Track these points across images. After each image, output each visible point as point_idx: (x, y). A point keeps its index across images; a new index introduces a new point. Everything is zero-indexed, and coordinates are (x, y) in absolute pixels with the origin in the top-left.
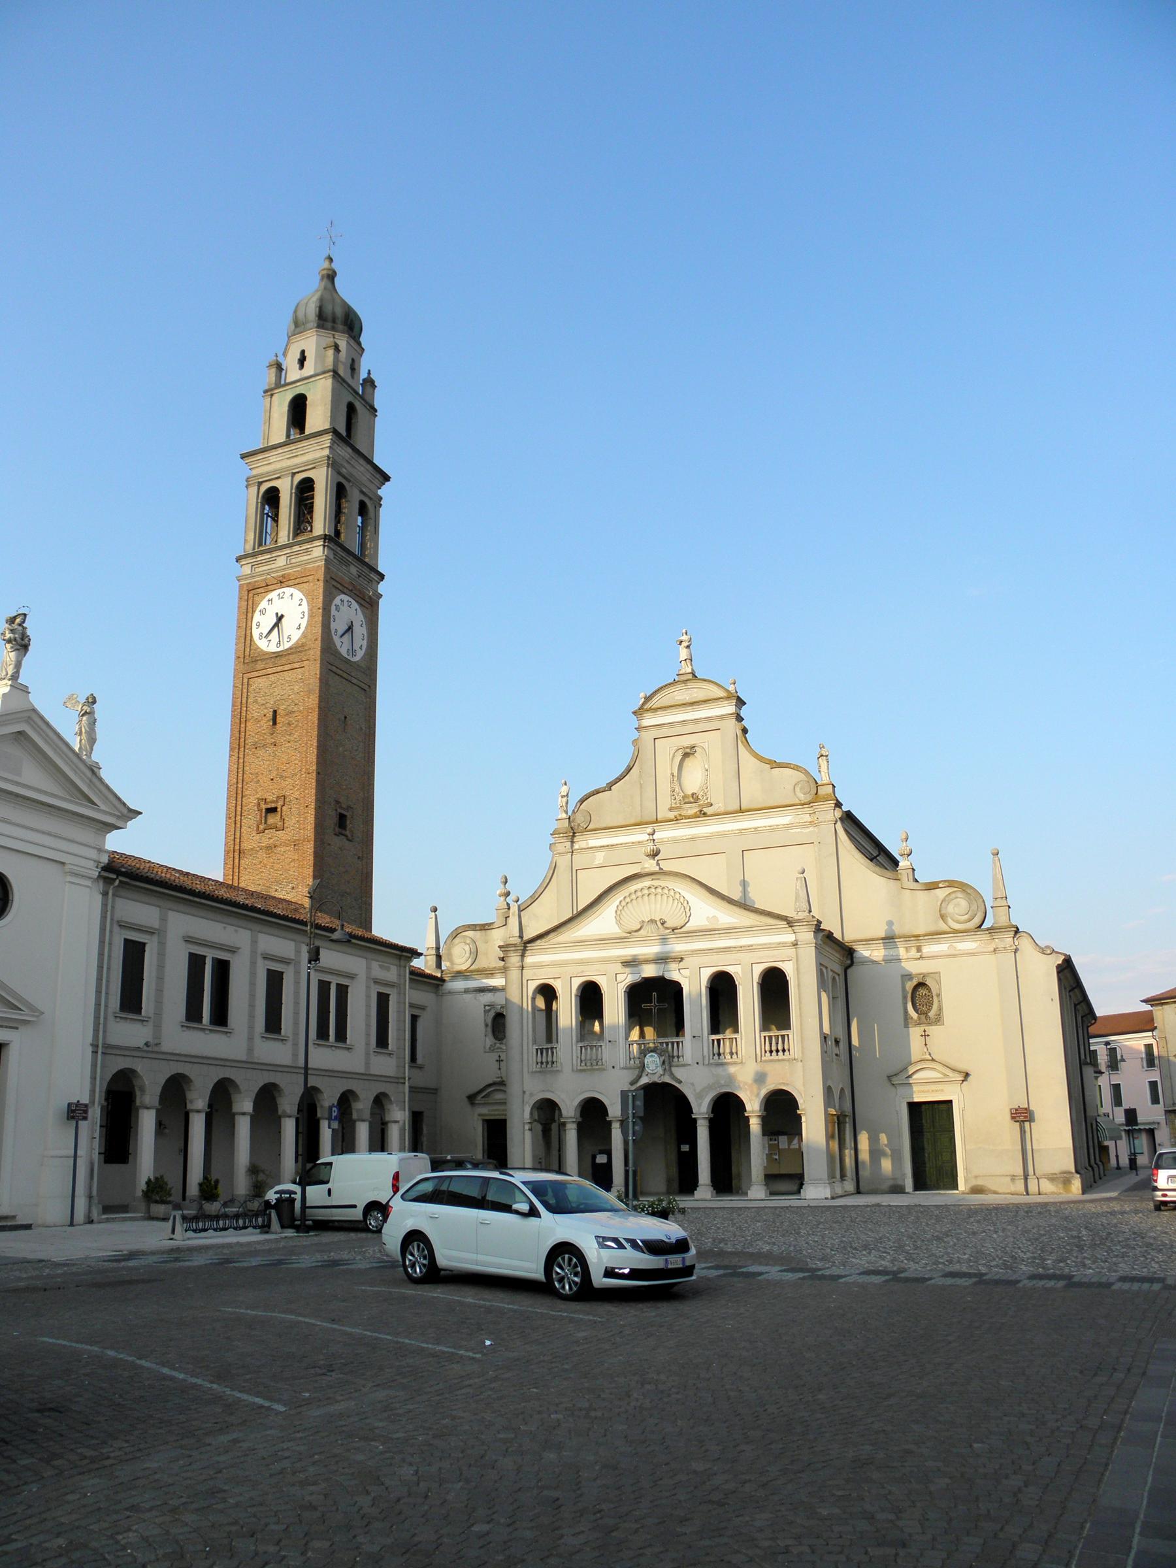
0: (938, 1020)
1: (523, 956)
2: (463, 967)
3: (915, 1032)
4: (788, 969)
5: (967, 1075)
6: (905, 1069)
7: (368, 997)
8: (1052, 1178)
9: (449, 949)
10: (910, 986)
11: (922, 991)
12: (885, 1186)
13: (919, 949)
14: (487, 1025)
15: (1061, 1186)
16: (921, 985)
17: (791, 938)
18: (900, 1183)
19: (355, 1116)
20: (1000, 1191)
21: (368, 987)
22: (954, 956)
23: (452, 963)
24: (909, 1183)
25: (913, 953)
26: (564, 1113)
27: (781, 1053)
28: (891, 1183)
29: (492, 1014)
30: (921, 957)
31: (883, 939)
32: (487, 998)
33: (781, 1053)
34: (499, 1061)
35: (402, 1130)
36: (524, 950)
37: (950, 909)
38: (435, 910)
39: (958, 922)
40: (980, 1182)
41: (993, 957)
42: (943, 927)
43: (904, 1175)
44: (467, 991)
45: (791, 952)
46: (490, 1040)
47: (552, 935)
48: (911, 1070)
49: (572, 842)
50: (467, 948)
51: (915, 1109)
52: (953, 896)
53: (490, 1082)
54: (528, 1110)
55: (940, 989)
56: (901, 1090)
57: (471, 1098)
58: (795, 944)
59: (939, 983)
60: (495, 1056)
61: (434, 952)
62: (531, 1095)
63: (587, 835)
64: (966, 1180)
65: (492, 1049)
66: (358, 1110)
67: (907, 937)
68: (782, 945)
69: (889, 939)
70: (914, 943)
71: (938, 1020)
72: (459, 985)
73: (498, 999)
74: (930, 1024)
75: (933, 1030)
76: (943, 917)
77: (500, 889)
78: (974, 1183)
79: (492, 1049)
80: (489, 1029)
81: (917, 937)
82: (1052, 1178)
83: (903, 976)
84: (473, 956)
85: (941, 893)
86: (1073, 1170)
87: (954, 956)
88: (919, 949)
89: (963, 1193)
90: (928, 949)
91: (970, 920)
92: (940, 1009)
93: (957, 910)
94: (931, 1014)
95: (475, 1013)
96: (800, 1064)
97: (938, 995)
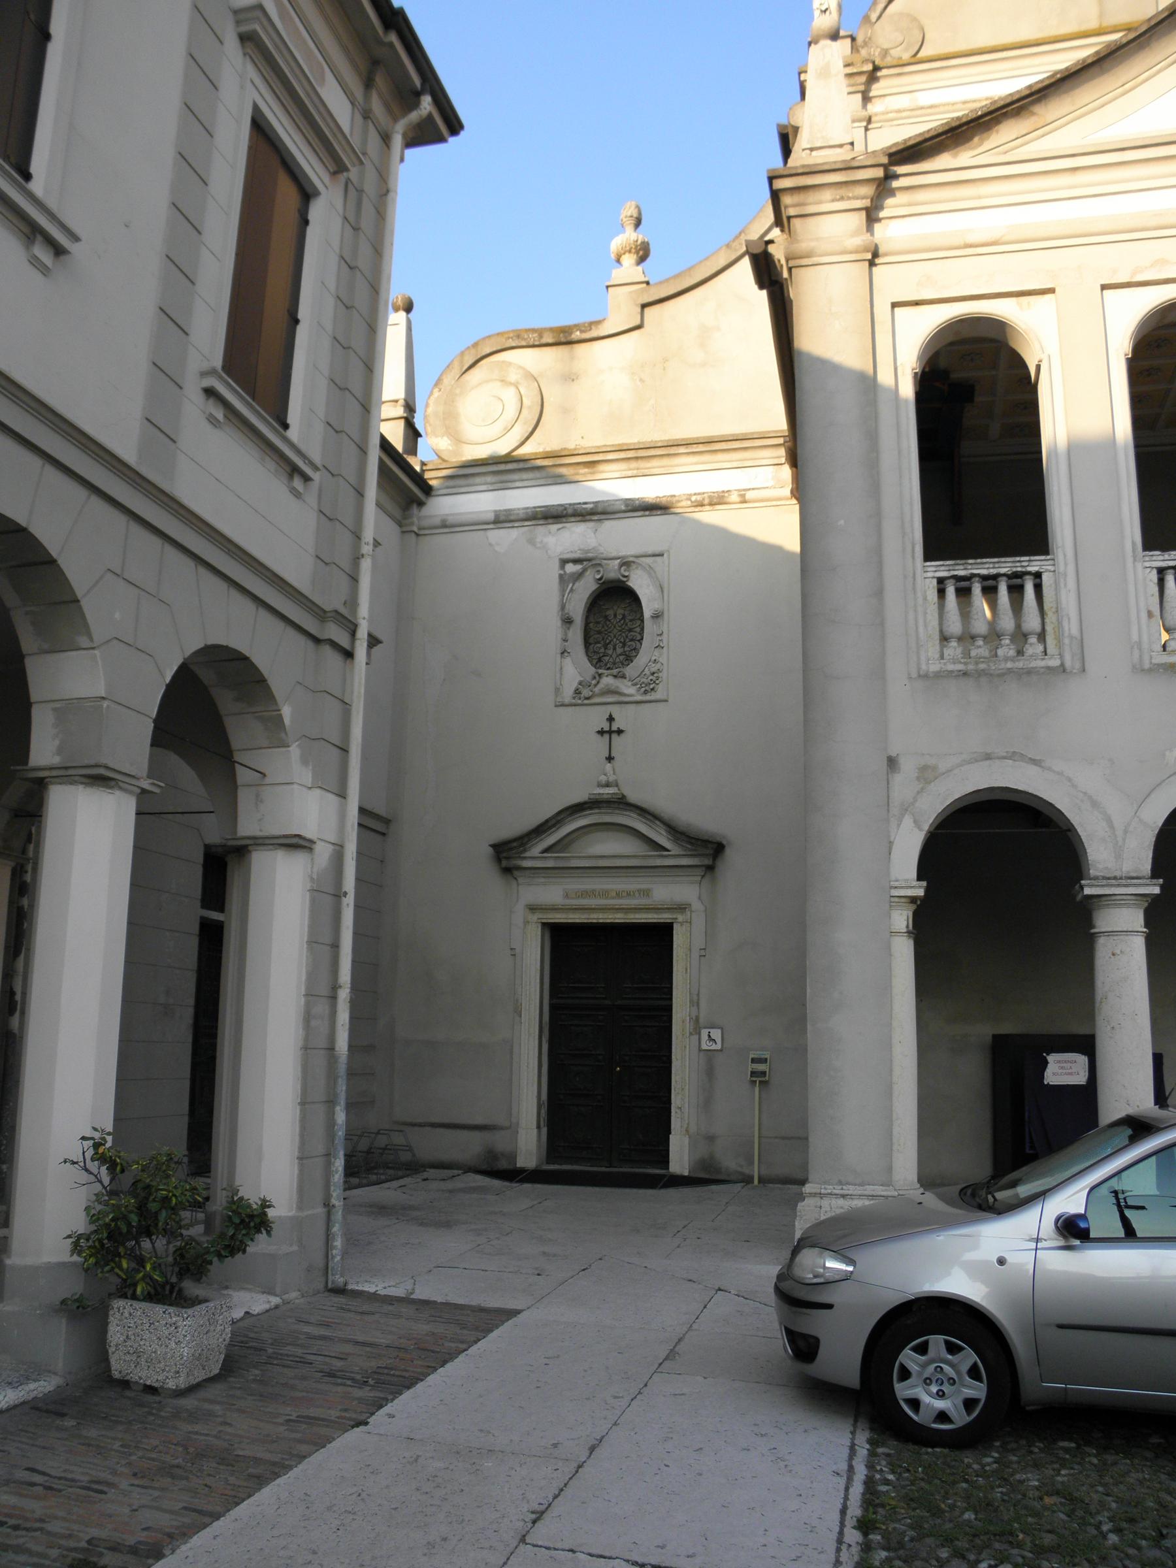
1: (872, 216)
2: (502, 448)
7: (196, 118)
9: (450, 401)
14: (568, 621)
19: (44, 750)
21: (201, 71)
23: (458, 440)
26: (1100, 856)
29: (587, 587)
32: (573, 538)
34: (610, 732)
35: (326, 895)
36: (884, 187)
38: (409, 308)
44: (502, 520)
46: (575, 669)
47: (1007, 132)
49: (866, 99)
50: (510, 396)
53: (579, 796)
54: (908, 844)
57: (507, 855)
60: (596, 718)
61: (400, 411)
62: (927, 775)
63: (915, 79)
65: (582, 697)
66: (67, 709)
72: (480, 502)
73: (614, 540)
77: (630, 236)
79: (582, 697)
80: (576, 634)
84: (530, 416)
95: (531, 584)
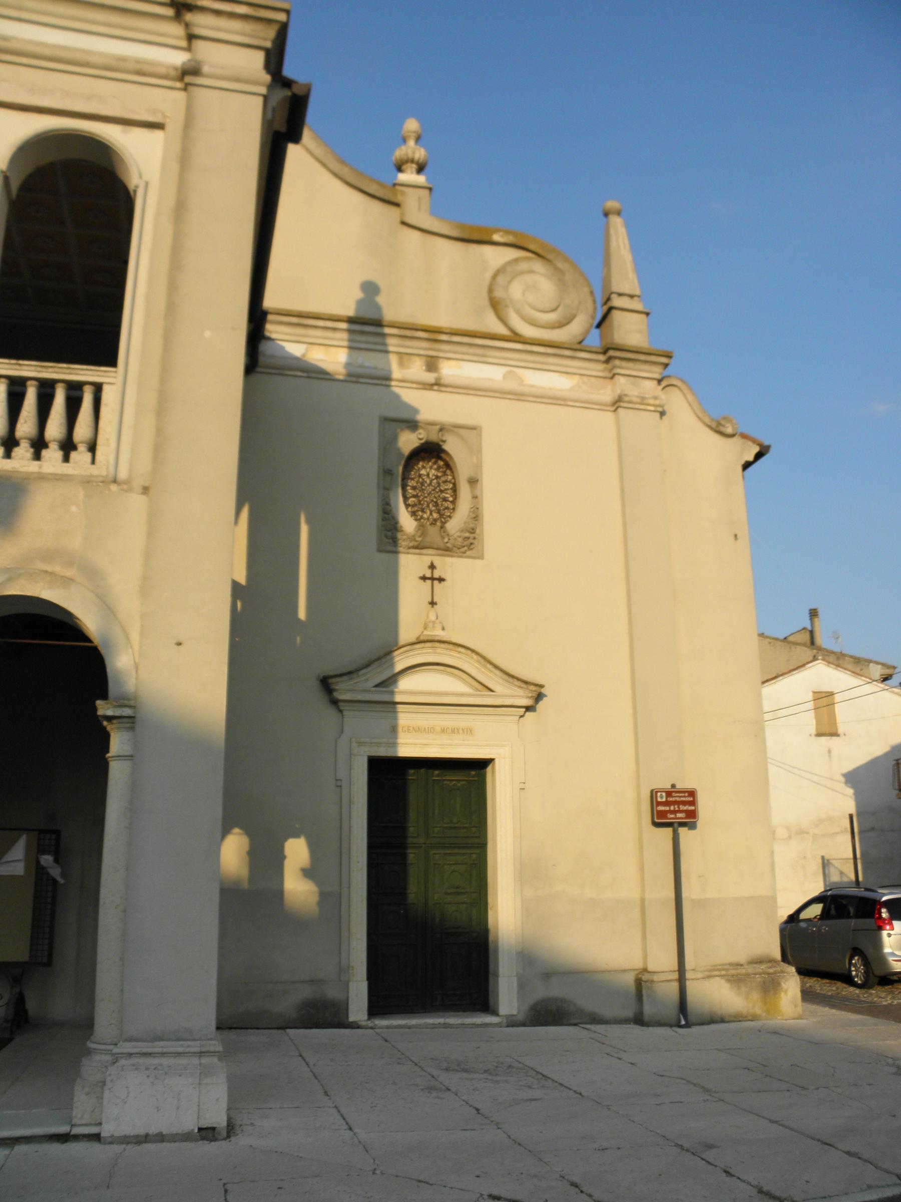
0: (468, 544)
3: (411, 566)
4: (144, 158)
5: (539, 697)
6: (386, 654)
8: (736, 975)
10: (408, 441)
11: (427, 470)
12: (287, 1004)
13: (432, 365)
15: (756, 996)
16: (430, 451)
17: (179, 58)
18: (333, 993)
20: (608, 1014)
22: (519, 396)
24: (358, 995)
25: (417, 370)
27: (52, 454)
28: (305, 993)
30: (438, 385)
31: (351, 320)
33: (52, 454)
37: (516, 291)
39: (533, 323)
40: (555, 991)
41: (608, 417)
42: (494, 325)
43: (343, 971)
45: (168, 102)
48: (401, 662)
51: (392, 778)
52: (524, 266)
55: (478, 466)
56: (354, 721)
58: (188, 74)
59: (476, 450)
64: (522, 986)
67: (409, 330)
68: (143, 73)
69: (366, 326)
70: (420, 347)
71: (468, 544)
74: (447, 551)
75: (448, 566)
76: (496, 305)
78: (540, 992)
81: (433, 334)
82: (736, 975)
83: (386, 420)
85: (495, 257)
86: (778, 955)
87: (519, 396)
88: (432, 365)
89: (512, 1023)
90: (450, 370)
91: (561, 325)
92: (476, 516)
93: (531, 297)
94: (456, 524)
96: (137, 503)
97: (473, 482)
